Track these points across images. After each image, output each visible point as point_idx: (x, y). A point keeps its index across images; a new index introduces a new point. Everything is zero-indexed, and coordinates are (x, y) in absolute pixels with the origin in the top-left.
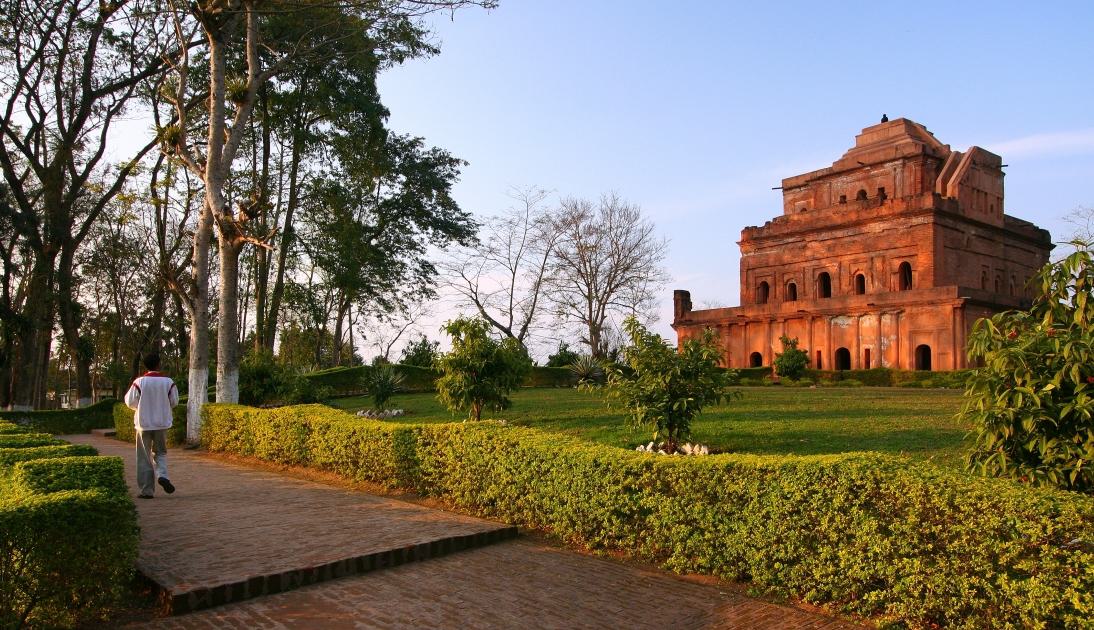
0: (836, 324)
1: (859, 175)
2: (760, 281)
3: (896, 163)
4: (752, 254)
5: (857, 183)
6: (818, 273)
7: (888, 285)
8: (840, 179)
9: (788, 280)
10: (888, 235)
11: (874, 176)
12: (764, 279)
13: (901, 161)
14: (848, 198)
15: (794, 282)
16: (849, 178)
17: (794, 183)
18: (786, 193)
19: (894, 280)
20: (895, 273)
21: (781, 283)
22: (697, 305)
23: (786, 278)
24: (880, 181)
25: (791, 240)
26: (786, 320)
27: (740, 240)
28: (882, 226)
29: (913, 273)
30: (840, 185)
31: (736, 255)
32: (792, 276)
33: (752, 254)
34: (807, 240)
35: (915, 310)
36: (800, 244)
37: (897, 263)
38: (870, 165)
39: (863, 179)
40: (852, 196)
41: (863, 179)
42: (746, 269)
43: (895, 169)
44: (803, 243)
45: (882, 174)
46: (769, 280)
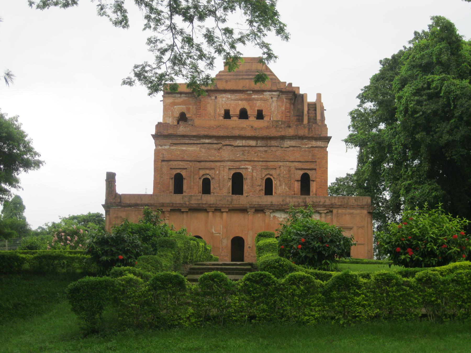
0: (274, 217)
1: (242, 96)
2: (175, 172)
3: (274, 93)
4: (167, 147)
5: (240, 102)
6: (233, 172)
8: (224, 95)
9: (203, 175)
10: (294, 150)
11: (254, 99)
12: (178, 171)
14: (231, 113)
15: (208, 177)
16: (234, 96)
18: (167, 95)
19: (297, 186)
20: (298, 181)
21: (196, 177)
22: (121, 189)
23: (202, 172)
24: (259, 105)
25: (207, 141)
26: (216, 210)
27: (154, 133)
28: (289, 142)
29: (311, 182)
30: (225, 101)
31: (151, 145)
32: (208, 172)
33: (167, 147)
34: (224, 143)
35: (340, 211)
36: (215, 146)
38: (253, 91)
39: (246, 100)
40: (235, 111)
42: (161, 161)
43: (272, 98)
44: (220, 146)
45: (261, 99)
46: (184, 173)
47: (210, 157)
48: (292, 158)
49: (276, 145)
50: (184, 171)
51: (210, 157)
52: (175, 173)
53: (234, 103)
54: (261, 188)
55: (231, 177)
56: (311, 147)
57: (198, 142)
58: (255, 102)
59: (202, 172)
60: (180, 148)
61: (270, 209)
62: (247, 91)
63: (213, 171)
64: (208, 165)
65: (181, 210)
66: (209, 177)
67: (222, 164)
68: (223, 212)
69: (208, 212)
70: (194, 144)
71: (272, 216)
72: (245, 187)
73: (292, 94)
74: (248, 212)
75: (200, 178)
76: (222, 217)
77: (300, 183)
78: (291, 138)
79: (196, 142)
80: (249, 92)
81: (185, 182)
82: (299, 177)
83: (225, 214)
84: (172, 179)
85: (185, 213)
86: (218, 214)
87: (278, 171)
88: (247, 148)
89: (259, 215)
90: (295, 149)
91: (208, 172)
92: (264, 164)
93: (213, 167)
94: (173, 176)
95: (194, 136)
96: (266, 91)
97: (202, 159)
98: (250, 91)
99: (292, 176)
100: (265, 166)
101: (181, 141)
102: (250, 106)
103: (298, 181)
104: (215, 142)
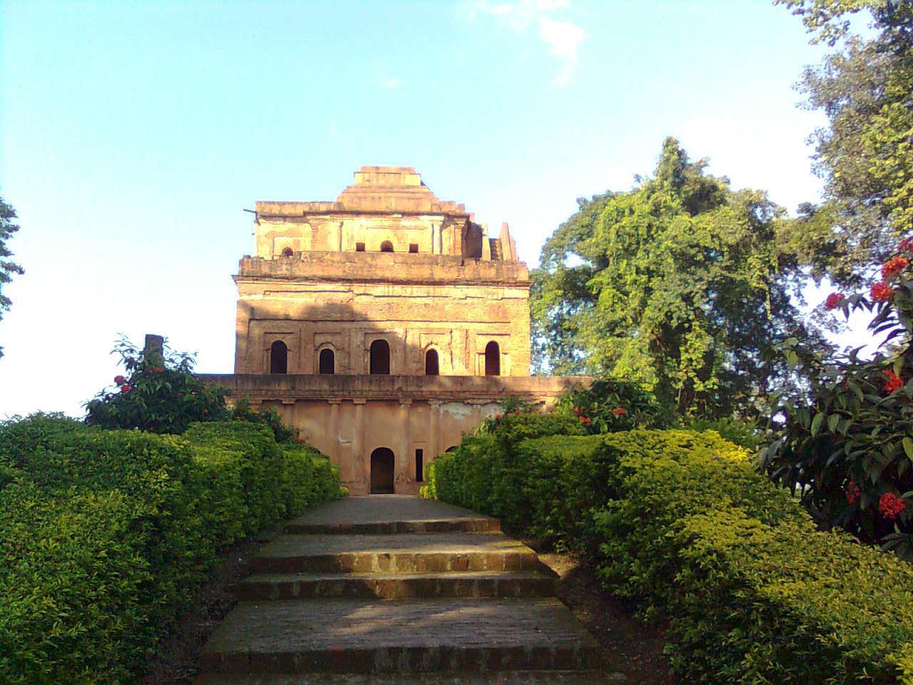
1: (386, 221)
7: (470, 367)
10: (473, 304)
12: (279, 338)
13: (442, 218)
17: (276, 210)
21: (310, 347)
23: (319, 339)
24: (412, 237)
29: (501, 356)
32: (329, 338)
34: (356, 291)
37: (482, 343)
39: (390, 227)
40: (373, 245)
41: (390, 227)
45: (416, 228)
46: (288, 341)
47: (333, 314)
48: (470, 319)
49: (444, 294)
50: (289, 337)
51: (333, 314)
52: (272, 341)
53: (370, 232)
54: (419, 366)
55: (369, 349)
56: (502, 299)
57: (312, 288)
58: (406, 231)
59: (319, 339)
60: (280, 297)
61: (440, 399)
62: (393, 213)
63: (338, 338)
64: (330, 325)
65: (281, 401)
66: (332, 348)
67: (354, 325)
68: (356, 405)
69: (331, 404)
70: (306, 291)
71: (442, 411)
72: (393, 365)
73: (465, 220)
74: (401, 404)
75: (316, 350)
76: (353, 415)
77: (484, 356)
78: (468, 283)
79: (308, 289)
80: (395, 216)
81: (289, 355)
82: (482, 348)
83: (359, 409)
84: (267, 350)
85: (289, 407)
86: (347, 409)
87: (446, 339)
88: (395, 300)
89: (420, 410)
90: (476, 301)
91: (329, 338)
92: (423, 325)
93: (339, 331)
94: (269, 346)
95: (306, 279)
96: (423, 214)
97: (320, 317)
98: (398, 213)
99: (472, 346)
100: (425, 329)
101: (284, 286)
102: (398, 239)
103: (480, 354)
104: (342, 288)
